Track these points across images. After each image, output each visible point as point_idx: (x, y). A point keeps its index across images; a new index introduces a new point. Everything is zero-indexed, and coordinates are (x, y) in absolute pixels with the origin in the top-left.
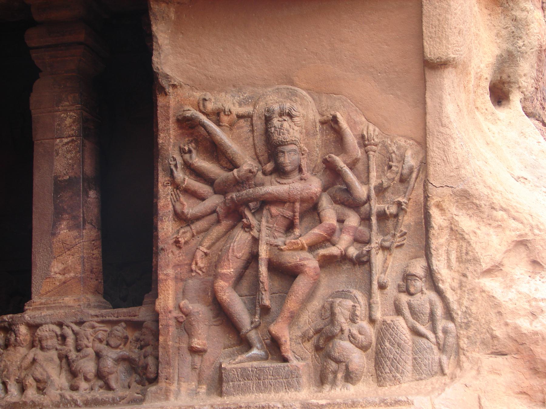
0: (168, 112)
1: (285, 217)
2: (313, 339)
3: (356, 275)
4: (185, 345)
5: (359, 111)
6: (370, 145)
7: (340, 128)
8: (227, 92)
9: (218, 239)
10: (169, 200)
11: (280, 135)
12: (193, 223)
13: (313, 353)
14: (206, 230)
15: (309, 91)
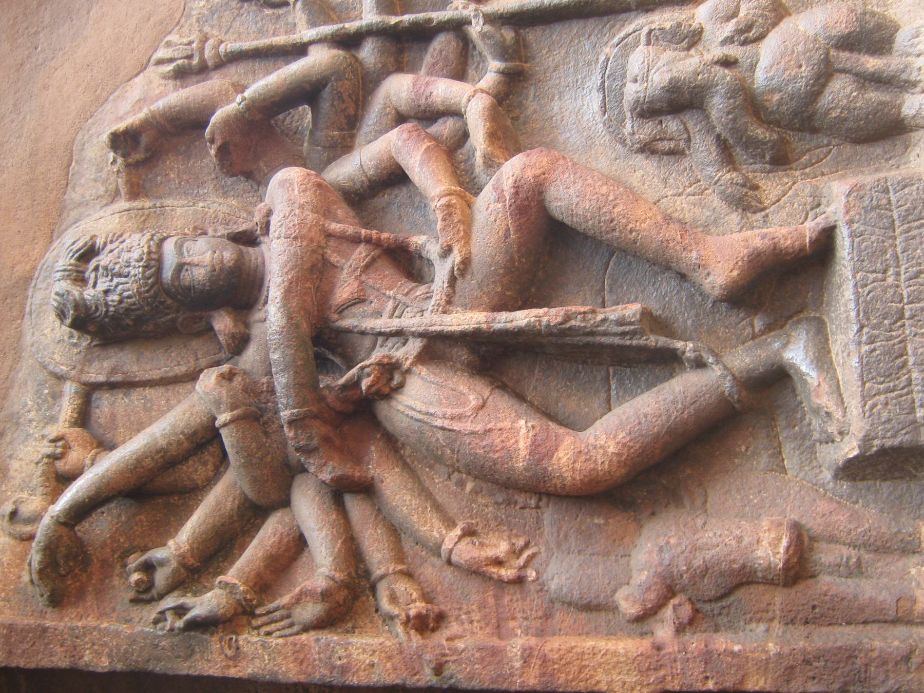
0: (27, 630)
1: (367, 267)
2: (751, 176)
3: (556, 68)
4: (778, 600)
5: (116, 94)
6: (202, 50)
7: (146, 124)
8: (10, 457)
9: (426, 494)
10: (280, 641)
11: (129, 273)
12: (367, 573)
13: (798, 173)
14: (395, 532)
15: (55, 234)
